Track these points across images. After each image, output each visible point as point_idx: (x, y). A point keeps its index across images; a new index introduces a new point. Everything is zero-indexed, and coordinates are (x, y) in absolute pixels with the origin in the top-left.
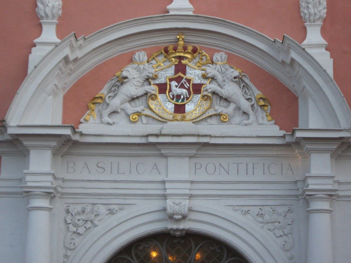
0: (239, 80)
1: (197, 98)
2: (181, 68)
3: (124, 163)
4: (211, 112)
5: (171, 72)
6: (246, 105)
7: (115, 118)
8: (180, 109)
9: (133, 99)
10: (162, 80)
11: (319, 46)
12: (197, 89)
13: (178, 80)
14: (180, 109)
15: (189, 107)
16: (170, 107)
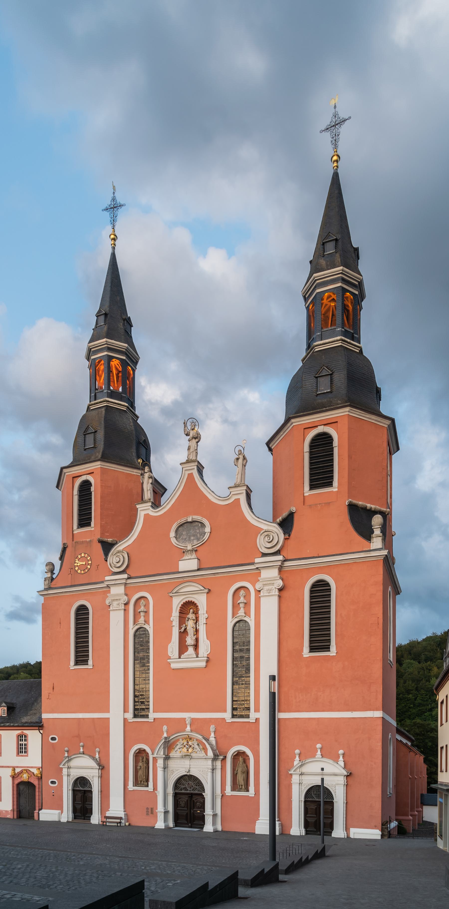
0: (198, 745)
1: (191, 748)
2: (188, 742)
3: (179, 761)
4: (193, 751)
5: (186, 743)
6: (199, 750)
7: (177, 752)
8: (188, 750)
9: (179, 748)
10: (184, 745)
11: (212, 737)
12: (191, 746)
13: (187, 744)
14: (188, 750)
15: (189, 750)
16: (186, 749)
